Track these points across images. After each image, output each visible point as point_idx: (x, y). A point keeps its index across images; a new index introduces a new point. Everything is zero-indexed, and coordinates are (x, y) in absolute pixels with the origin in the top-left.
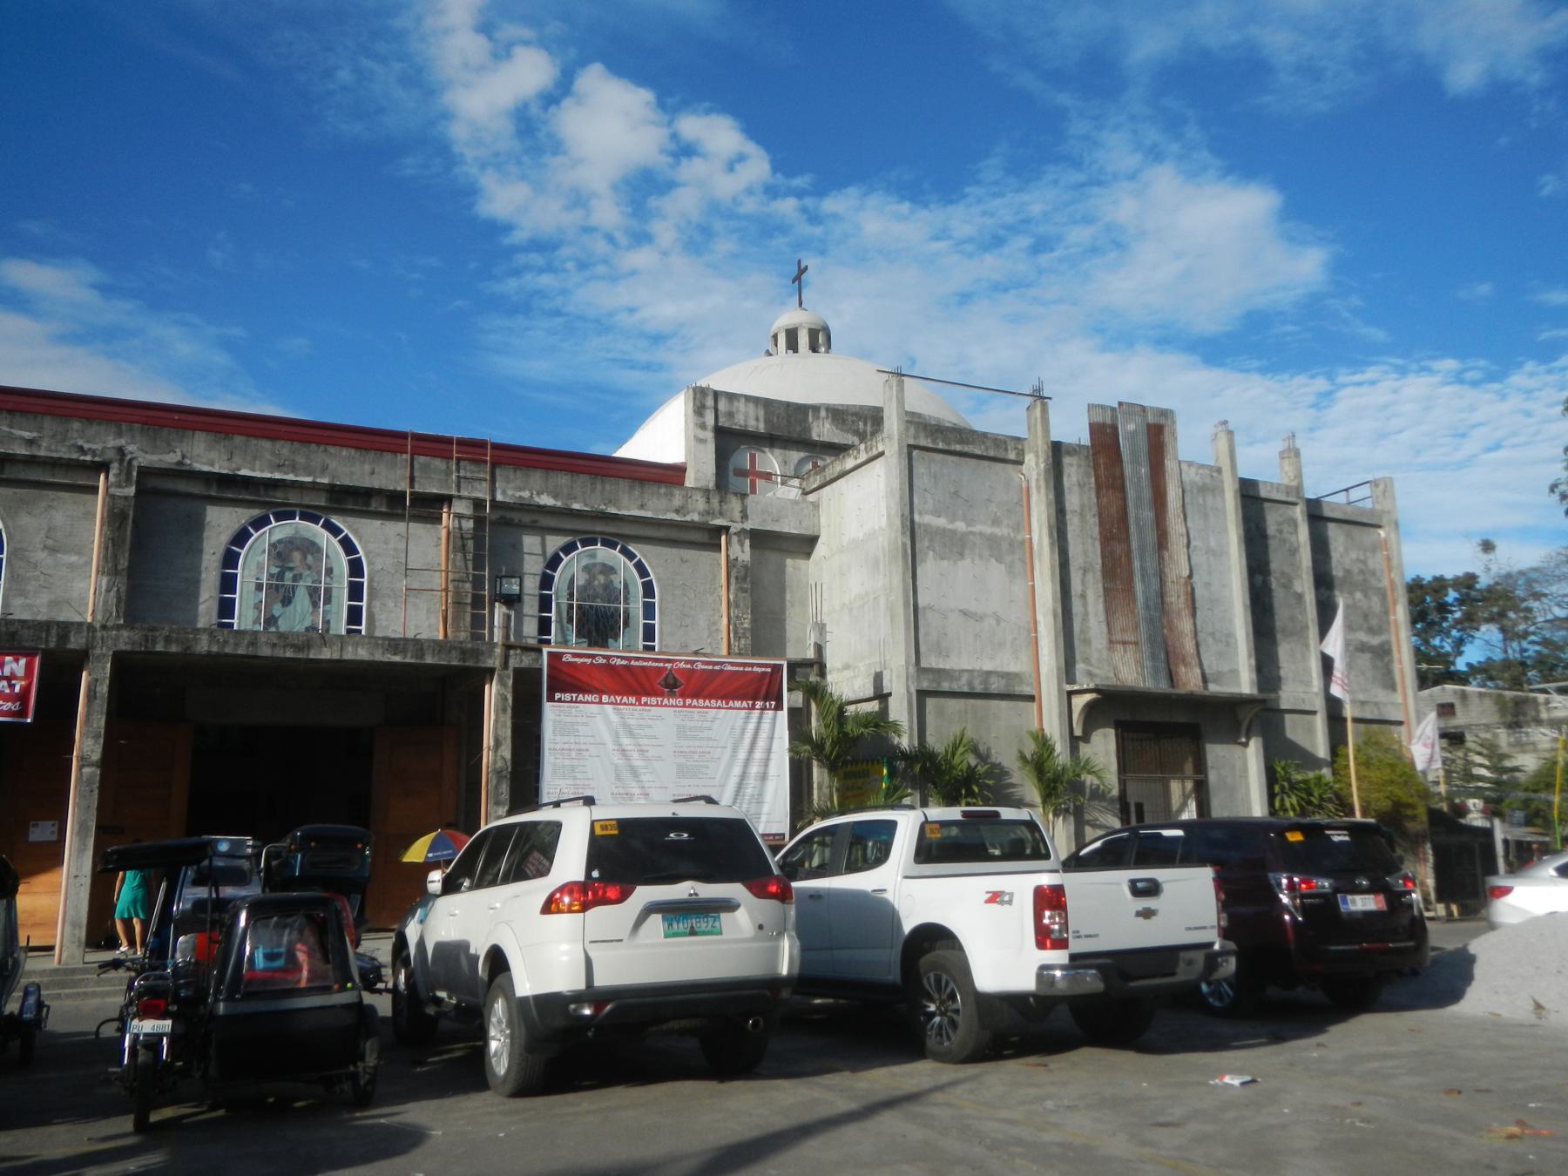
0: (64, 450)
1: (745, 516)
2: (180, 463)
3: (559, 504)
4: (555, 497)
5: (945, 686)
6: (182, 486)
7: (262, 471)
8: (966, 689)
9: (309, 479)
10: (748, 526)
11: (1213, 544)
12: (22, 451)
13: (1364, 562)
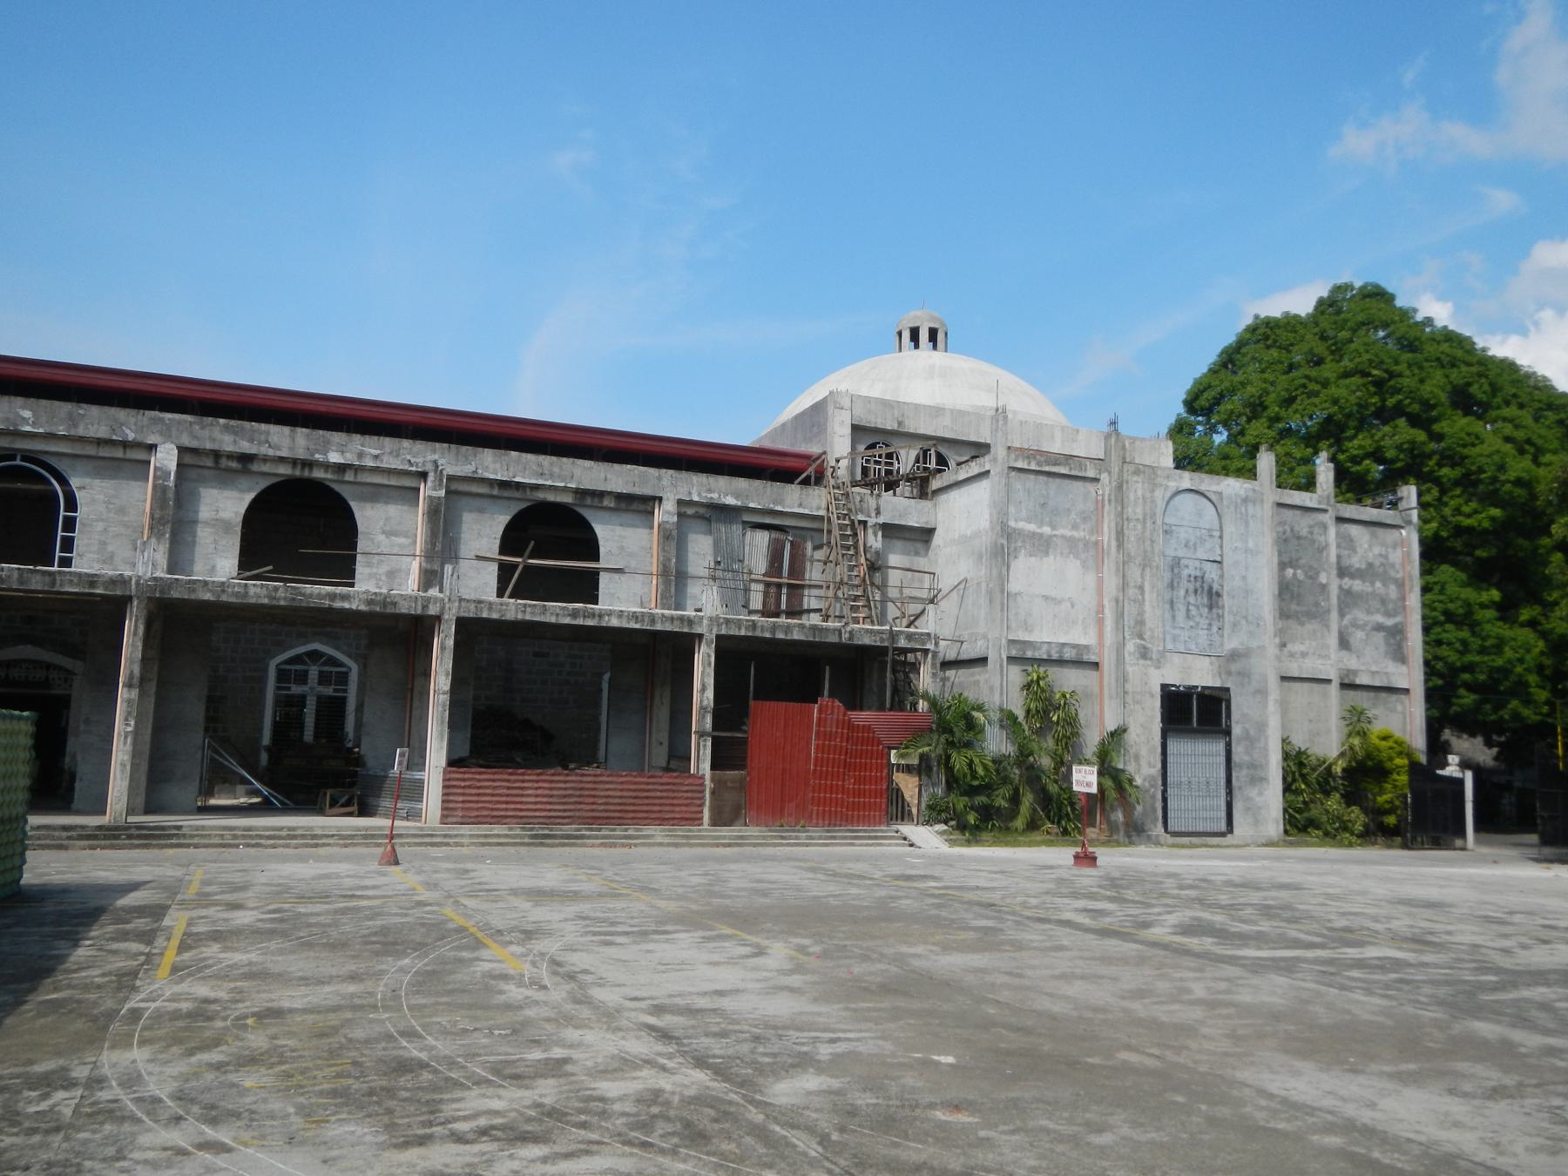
1: (878, 512)
2: (476, 472)
3: (739, 503)
4: (737, 498)
5: (1029, 654)
6: (475, 489)
8: (1045, 657)
9: (562, 484)
10: (881, 520)
11: (1251, 544)
12: (370, 463)
13: (1386, 557)
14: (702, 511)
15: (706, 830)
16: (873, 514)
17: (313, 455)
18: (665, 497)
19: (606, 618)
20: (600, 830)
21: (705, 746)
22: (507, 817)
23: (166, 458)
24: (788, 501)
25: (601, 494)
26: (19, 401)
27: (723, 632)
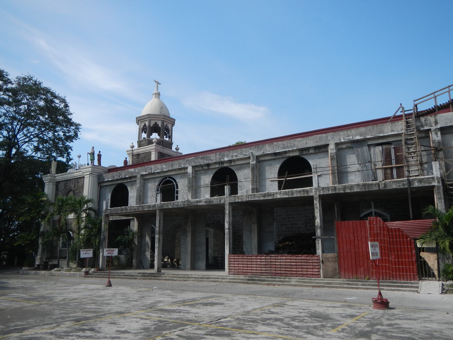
0: (242, 156)
1: (436, 123)
2: (264, 153)
3: (362, 138)
4: (361, 136)
6: (267, 158)
7: (281, 150)
9: (291, 149)
10: (439, 126)
12: (235, 158)
14: (349, 145)
15: (322, 280)
16: (434, 125)
17: (221, 160)
18: (330, 144)
19: (276, 195)
20: (275, 278)
21: (318, 243)
22: (247, 272)
23: (190, 170)
24: (386, 130)
25: (308, 149)
26: (163, 164)
27: (322, 193)
